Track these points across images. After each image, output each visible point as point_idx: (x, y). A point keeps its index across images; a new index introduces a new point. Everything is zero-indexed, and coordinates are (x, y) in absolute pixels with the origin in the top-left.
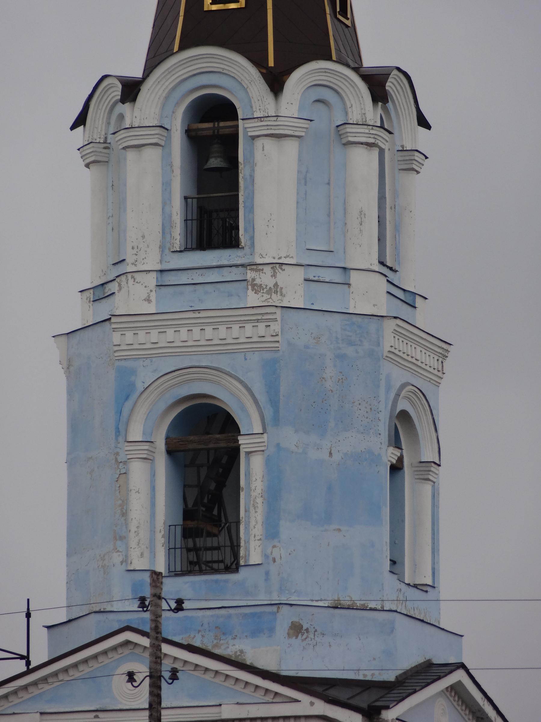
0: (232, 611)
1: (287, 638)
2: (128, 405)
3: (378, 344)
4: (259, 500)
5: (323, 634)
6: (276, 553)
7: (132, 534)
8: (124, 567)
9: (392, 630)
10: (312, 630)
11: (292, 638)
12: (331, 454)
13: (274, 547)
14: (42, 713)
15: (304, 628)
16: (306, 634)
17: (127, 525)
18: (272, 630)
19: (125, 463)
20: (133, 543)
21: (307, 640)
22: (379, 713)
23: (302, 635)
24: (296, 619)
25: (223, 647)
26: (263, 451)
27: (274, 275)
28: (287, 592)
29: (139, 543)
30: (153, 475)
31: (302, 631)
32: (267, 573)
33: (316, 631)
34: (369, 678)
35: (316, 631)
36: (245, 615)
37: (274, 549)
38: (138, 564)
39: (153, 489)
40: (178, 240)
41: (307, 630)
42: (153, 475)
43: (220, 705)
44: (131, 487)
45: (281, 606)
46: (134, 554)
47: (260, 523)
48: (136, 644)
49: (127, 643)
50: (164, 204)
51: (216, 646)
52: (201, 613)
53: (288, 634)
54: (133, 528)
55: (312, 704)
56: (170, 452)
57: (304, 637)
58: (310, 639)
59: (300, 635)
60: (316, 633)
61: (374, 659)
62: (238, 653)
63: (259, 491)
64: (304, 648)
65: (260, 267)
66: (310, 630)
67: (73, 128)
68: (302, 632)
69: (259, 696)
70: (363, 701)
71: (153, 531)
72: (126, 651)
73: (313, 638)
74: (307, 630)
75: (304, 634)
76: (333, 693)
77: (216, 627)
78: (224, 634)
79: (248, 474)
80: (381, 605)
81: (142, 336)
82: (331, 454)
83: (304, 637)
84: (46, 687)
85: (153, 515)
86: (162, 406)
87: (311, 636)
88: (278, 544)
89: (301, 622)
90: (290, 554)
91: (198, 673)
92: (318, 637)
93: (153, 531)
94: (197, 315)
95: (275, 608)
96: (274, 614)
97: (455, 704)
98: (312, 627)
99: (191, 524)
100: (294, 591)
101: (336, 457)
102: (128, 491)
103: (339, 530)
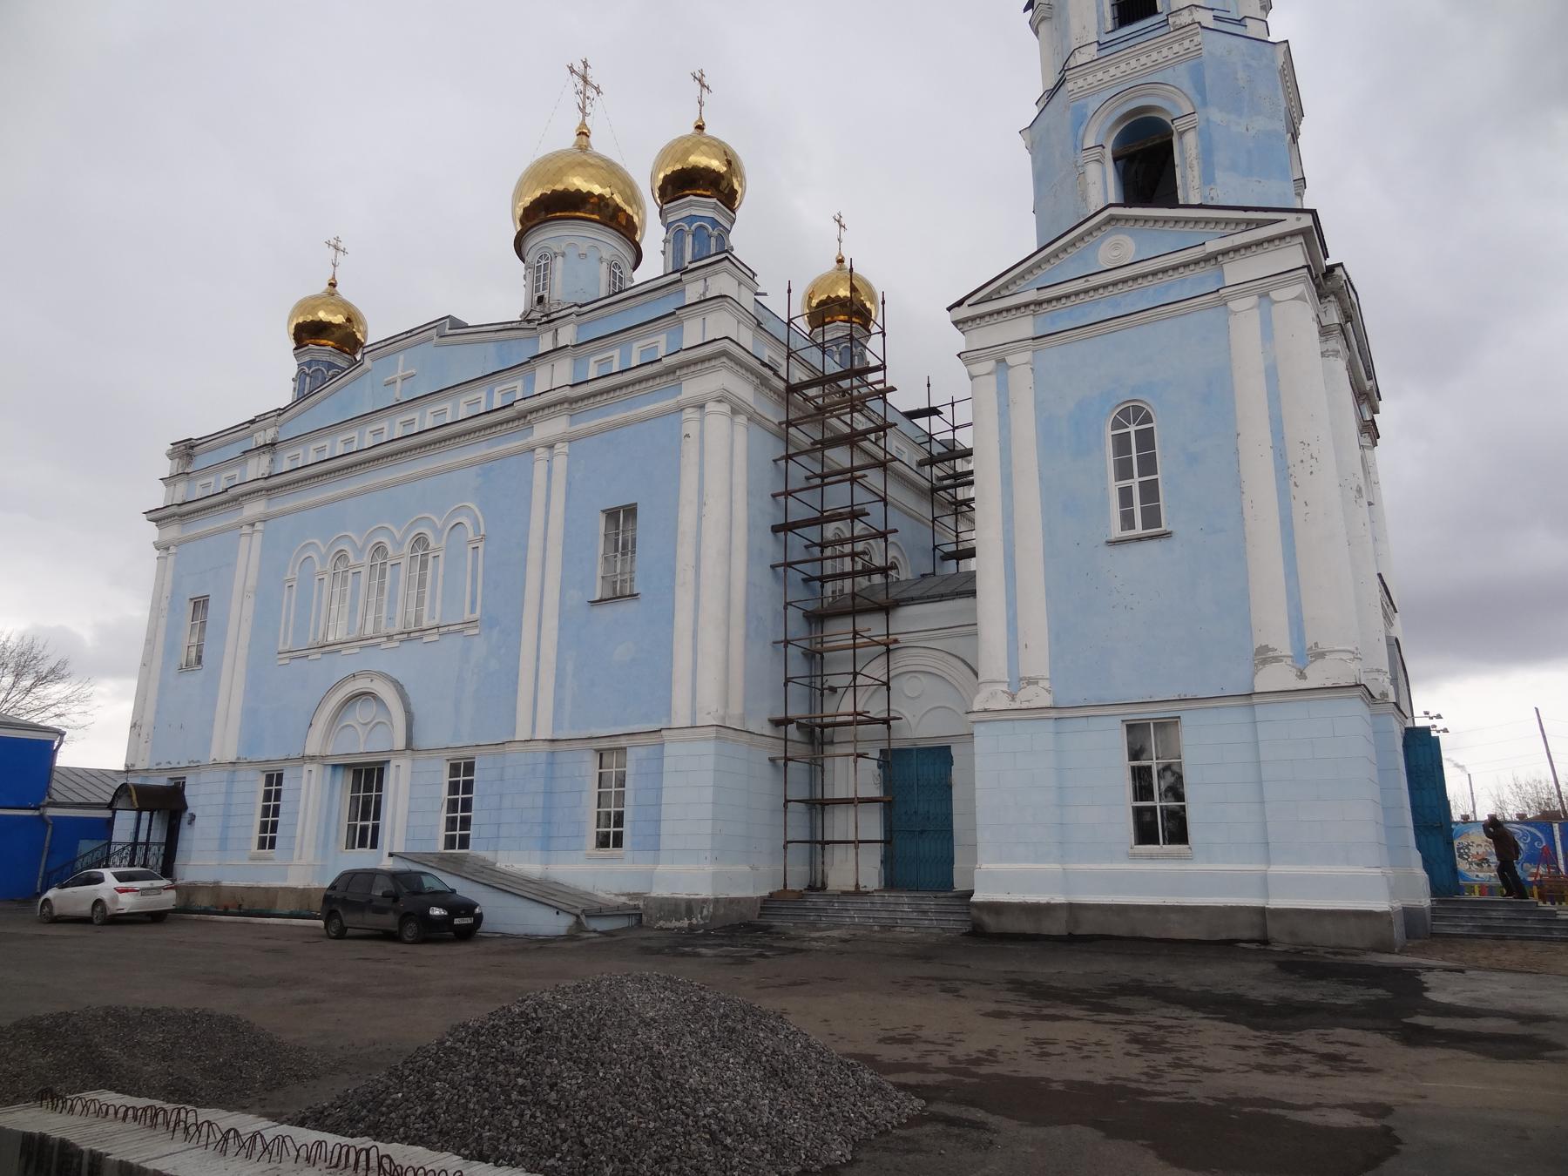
2: (1083, 128)
3: (1274, 62)
4: (1195, 162)
12: (1247, 130)
13: (1212, 189)
19: (1083, 166)
22: (1334, 270)
26: (1195, 127)
27: (1191, 14)
37: (1212, 192)
39: (1105, 183)
40: (1109, 25)
43: (1204, 243)
47: (1197, 177)
50: (1098, 6)
56: (1115, 160)
63: (1194, 155)
65: (1179, 13)
67: (1025, 10)
79: (1182, 152)
81: (1090, 79)
82: (1247, 130)
84: (1040, 272)
86: (1109, 123)
94: (1133, 49)
101: (1252, 132)
103: (1260, 182)
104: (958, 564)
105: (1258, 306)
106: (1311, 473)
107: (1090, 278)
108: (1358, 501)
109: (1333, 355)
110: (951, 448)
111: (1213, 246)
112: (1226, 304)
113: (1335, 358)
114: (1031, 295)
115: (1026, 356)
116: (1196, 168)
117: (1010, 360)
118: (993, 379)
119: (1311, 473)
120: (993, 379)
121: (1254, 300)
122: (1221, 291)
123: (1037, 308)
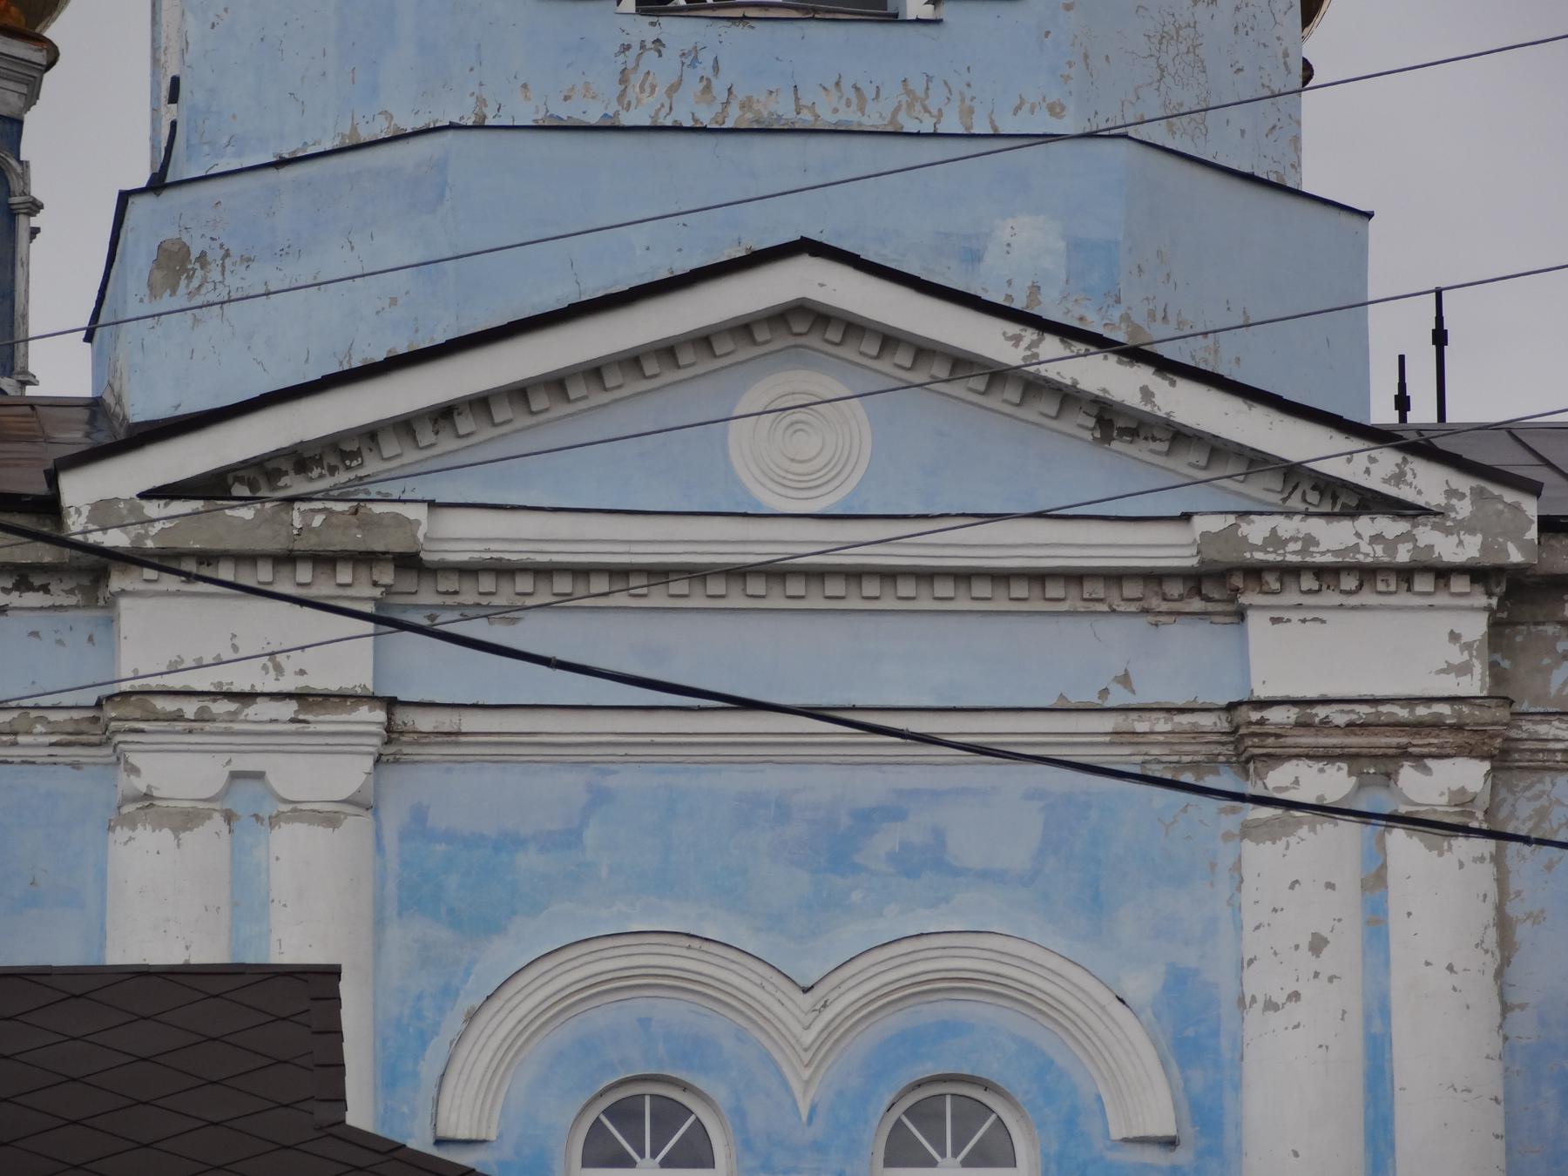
1: (146, 300)
5: (249, 260)
10: (215, 255)
11: (161, 297)
15: (195, 254)
16: (199, 273)
21: (203, 291)
23: (190, 278)
24: (170, 233)
28: (206, 148)
31: (190, 266)
33: (227, 254)
35: (227, 254)
41: (203, 258)
53: (150, 286)
57: (195, 283)
58: (211, 286)
59: (183, 283)
60: (228, 262)
61: (394, 301)
66: (209, 258)
68: (187, 270)
73: (221, 279)
75: (194, 274)
80: (476, 114)
83: (195, 283)
87: (215, 274)
89: (186, 239)
90: (213, 26)
92: (232, 272)
98: (216, 245)
100: (225, 140)
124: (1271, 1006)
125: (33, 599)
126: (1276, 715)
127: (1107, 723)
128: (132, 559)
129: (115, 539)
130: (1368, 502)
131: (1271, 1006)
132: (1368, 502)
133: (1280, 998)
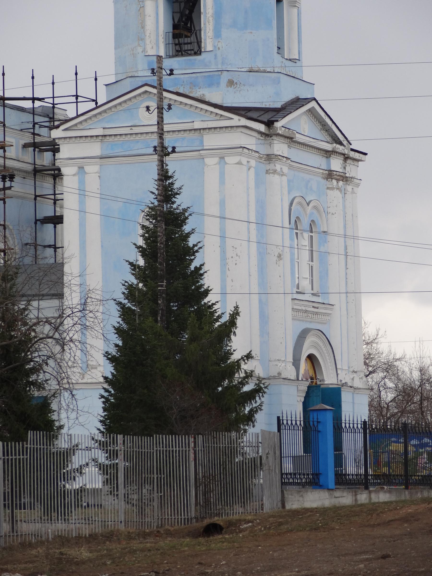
0: (198, 75)
4: (211, 19)
6: (220, 45)
7: (147, 37)
8: (143, 54)
9: (279, 82)
10: (238, 83)
13: (219, 42)
14: (103, 128)
17: (144, 32)
18: (218, 84)
20: (148, 42)
22: (273, 124)
24: (230, 78)
25: (194, 93)
29: (151, 42)
30: (157, 7)
32: (216, 55)
34: (267, 106)
35: (241, 83)
36: (205, 76)
37: (219, 43)
38: (151, 52)
39: (157, 14)
41: (236, 83)
42: (157, 7)
44: (146, 13)
45: (223, 71)
46: (148, 47)
47: (211, 30)
48: (150, 93)
49: (146, 92)
51: (191, 92)
52: (182, 76)
54: (148, 35)
55: (239, 120)
59: (233, 86)
61: (270, 97)
62: (202, 96)
64: (235, 92)
69: (213, 117)
70: (265, 118)
71: (157, 36)
72: (146, 96)
74: (236, 83)
76: (250, 114)
77: (191, 83)
78: (195, 86)
83: (235, 87)
85: (157, 28)
87: (238, 86)
88: (220, 40)
91: (181, 106)
93: (157, 36)
95: (220, 73)
96: (219, 75)
97: (311, 118)
99: (177, 31)
102: (145, 15)
103: (251, 33)
104: (55, 227)
105: (219, 163)
106: (236, 264)
107: (133, 128)
108: (278, 262)
109: (272, 173)
110: (51, 116)
111: (197, 125)
112: (203, 159)
113: (273, 175)
114: (100, 132)
115: (96, 168)
116: (211, 23)
117: (87, 169)
118: (76, 178)
119: (236, 264)
120: (76, 178)
121: (216, 160)
122: (201, 152)
123: (103, 138)
124: (333, 214)
125: (262, 138)
126: (335, 173)
127: (322, 171)
128: (278, 135)
129: (280, 132)
130: (341, 143)
131: (333, 214)
132: (341, 143)
133: (334, 213)
